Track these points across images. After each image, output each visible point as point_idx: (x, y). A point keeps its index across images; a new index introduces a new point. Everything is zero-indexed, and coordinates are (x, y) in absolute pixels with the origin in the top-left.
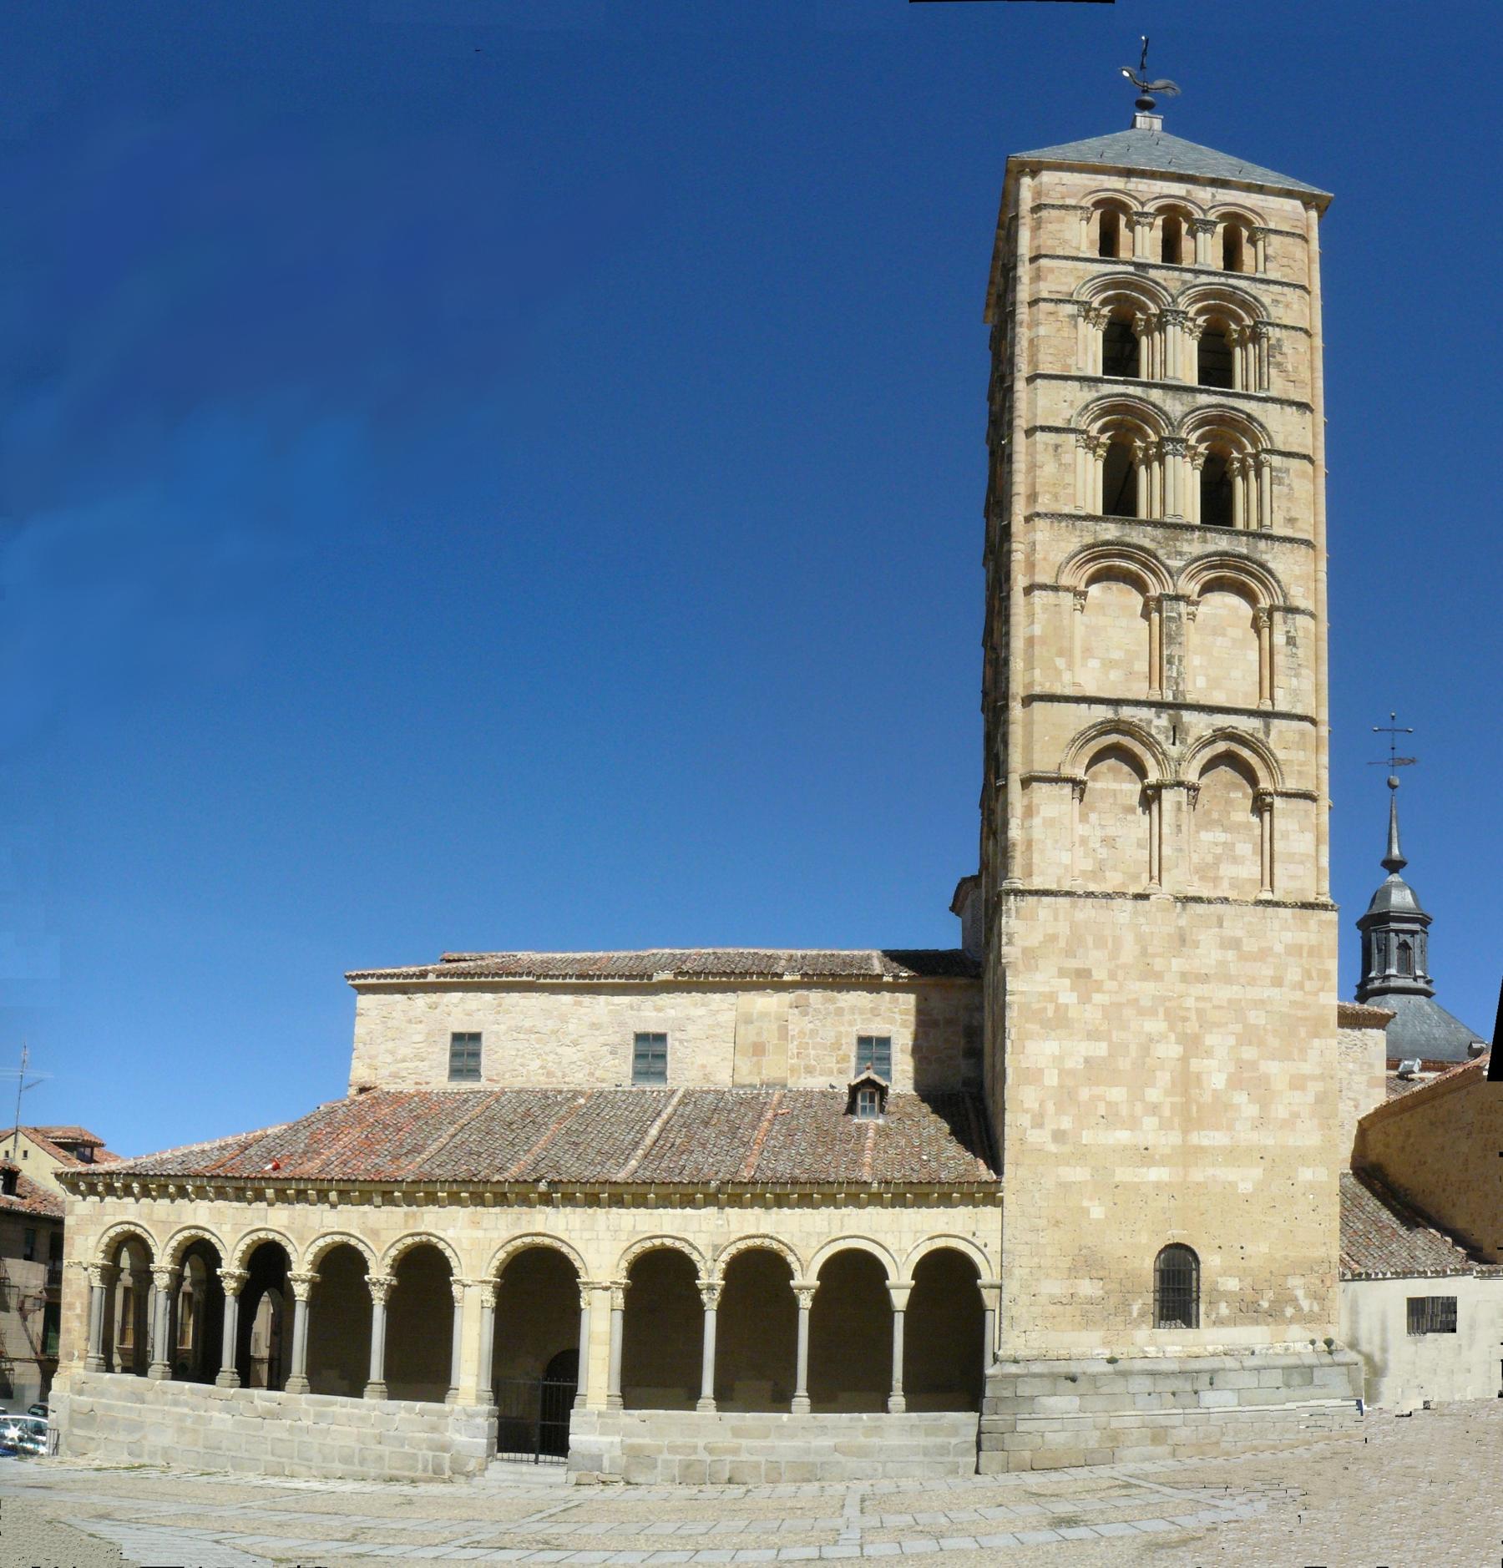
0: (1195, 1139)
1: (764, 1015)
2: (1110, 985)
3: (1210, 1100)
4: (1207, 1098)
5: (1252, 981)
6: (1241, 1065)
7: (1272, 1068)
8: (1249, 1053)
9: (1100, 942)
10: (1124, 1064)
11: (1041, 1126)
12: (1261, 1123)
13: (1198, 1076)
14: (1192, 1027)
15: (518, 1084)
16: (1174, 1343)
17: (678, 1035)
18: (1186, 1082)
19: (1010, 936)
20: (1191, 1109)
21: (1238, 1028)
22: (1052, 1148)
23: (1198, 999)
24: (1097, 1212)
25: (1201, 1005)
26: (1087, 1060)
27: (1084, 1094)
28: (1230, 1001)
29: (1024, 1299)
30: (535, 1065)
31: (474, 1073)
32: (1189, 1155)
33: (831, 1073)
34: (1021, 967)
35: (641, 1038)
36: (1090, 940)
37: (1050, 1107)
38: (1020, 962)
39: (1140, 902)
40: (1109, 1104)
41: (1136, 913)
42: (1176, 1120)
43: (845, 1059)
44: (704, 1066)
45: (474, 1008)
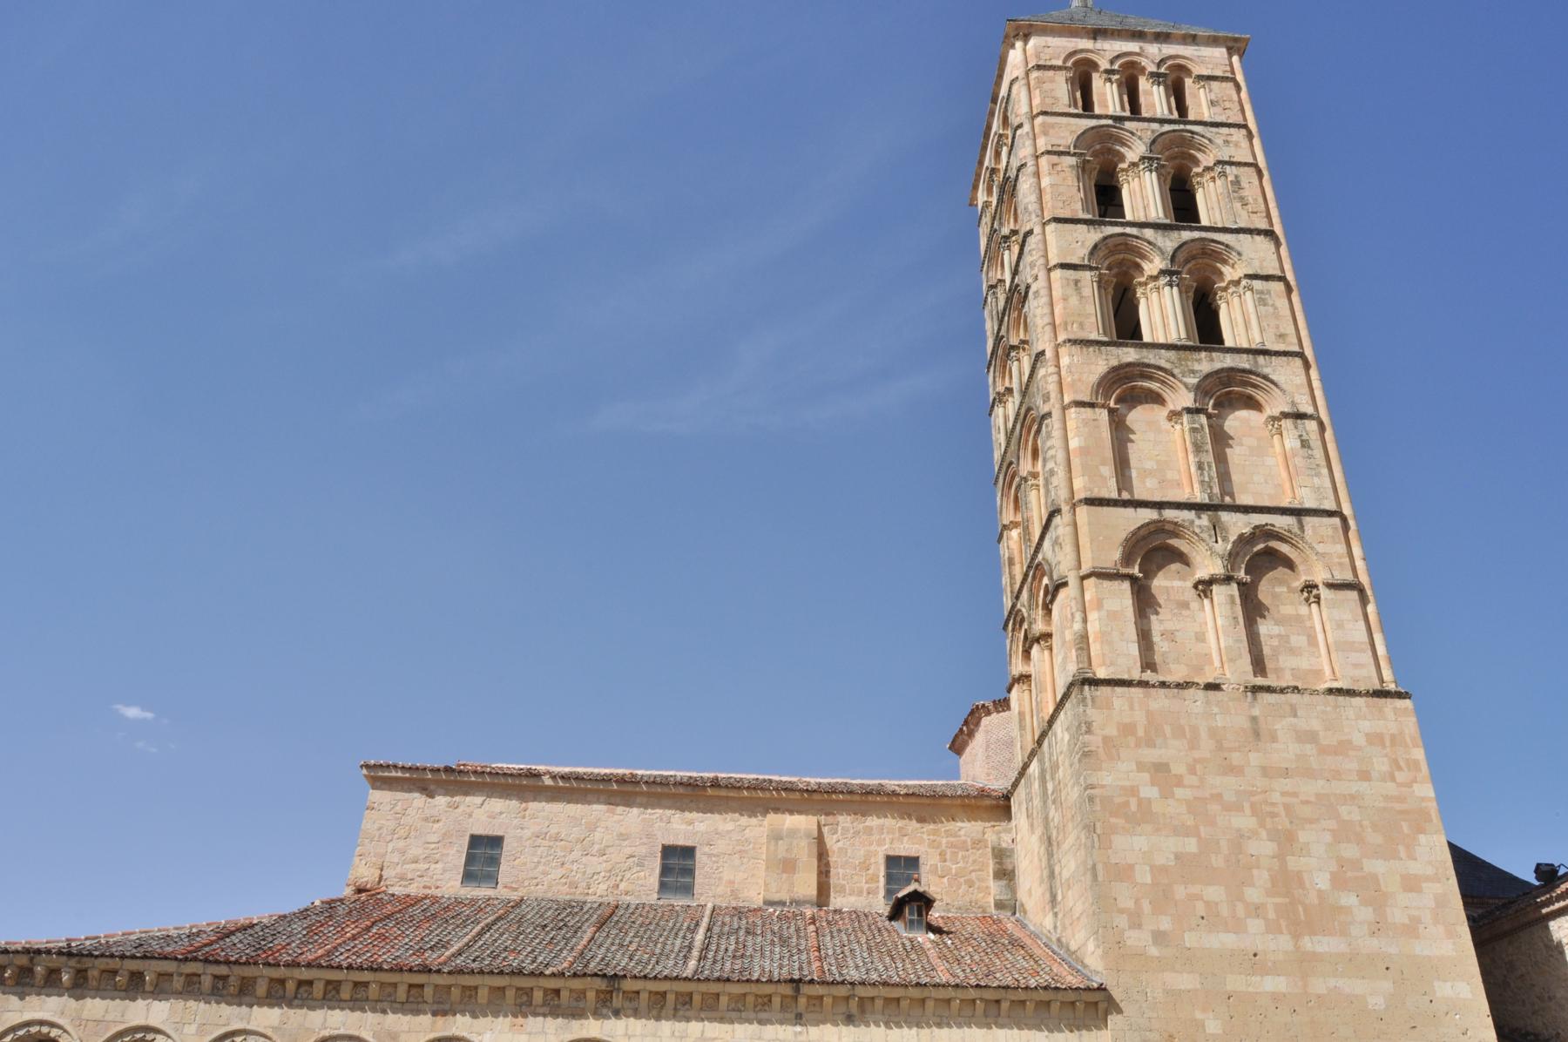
0: (1307, 943)
1: (793, 833)
3: (1316, 901)
4: (1313, 899)
5: (1337, 775)
6: (1342, 863)
7: (1376, 866)
8: (1350, 851)
9: (1179, 732)
10: (1217, 861)
11: (1140, 926)
12: (1377, 928)
13: (1299, 874)
14: (1283, 822)
15: (540, 892)
17: (707, 849)
20: (1299, 914)
21: (1332, 824)
22: (1154, 951)
23: (1283, 794)
24: (1213, 1026)
25: (1287, 800)
26: (1177, 856)
27: (1180, 892)
28: (1318, 795)
30: (557, 873)
31: (492, 879)
32: (1305, 963)
33: (860, 893)
35: (668, 851)
36: (1168, 729)
37: (1146, 907)
38: (1101, 750)
39: (1211, 693)
40: (1207, 903)
41: (1208, 702)
42: (1283, 923)
43: (874, 879)
44: (731, 882)
45: (498, 810)
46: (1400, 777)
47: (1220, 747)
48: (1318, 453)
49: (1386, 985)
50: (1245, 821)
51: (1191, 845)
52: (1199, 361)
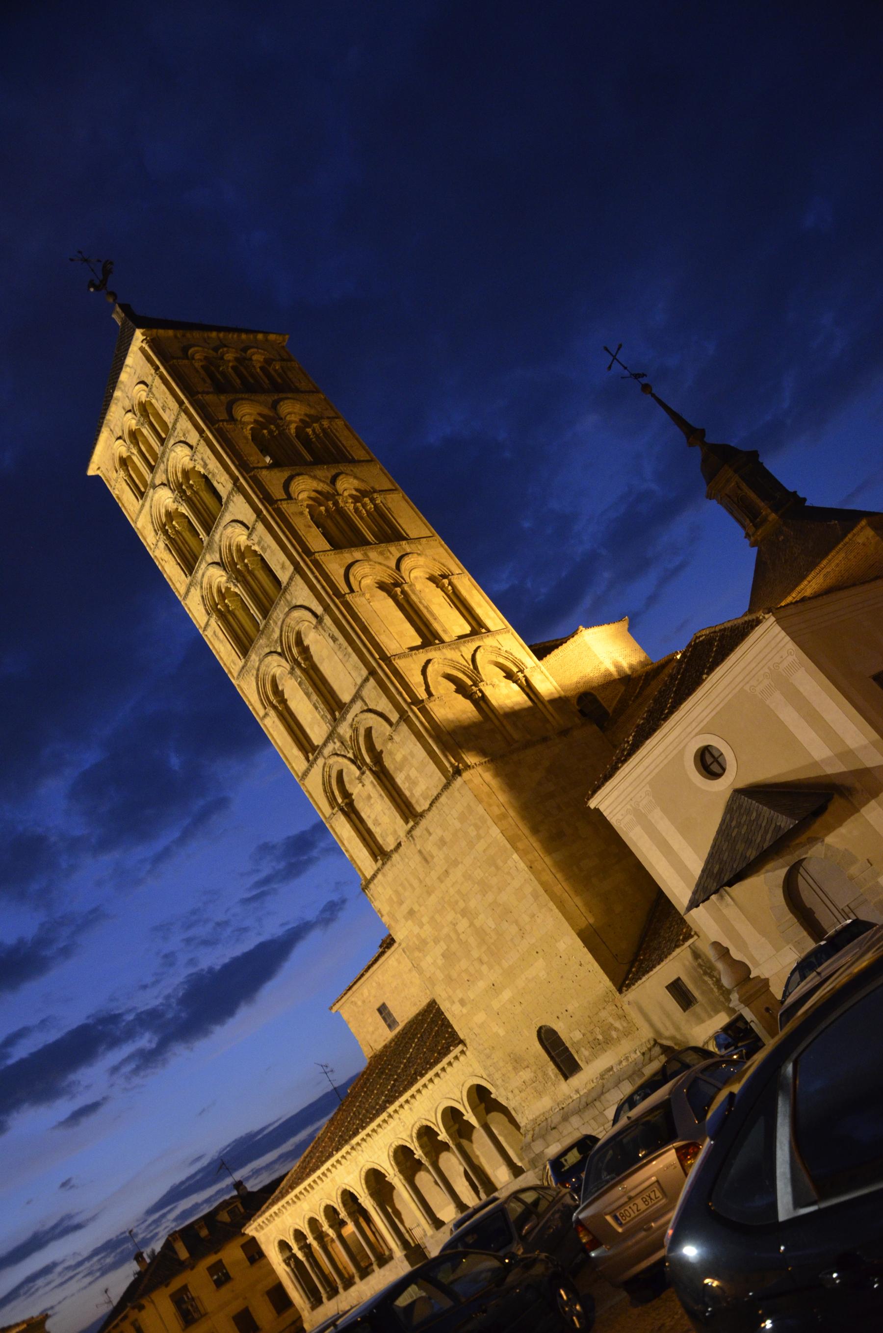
2: (423, 908)
8: (490, 897)
14: (462, 904)
16: (579, 1081)
18: (481, 934)
19: (379, 911)
22: (465, 1011)
27: (454, 975)
29: (510, 1096)
34: (393, 924)
41: (402, 859)
46: (482, 832)
47: (421, 882)
48: (341, 639)
49: (540, 963)
50: (450, 916)
51: (442, 946)
52: (273, 631)
